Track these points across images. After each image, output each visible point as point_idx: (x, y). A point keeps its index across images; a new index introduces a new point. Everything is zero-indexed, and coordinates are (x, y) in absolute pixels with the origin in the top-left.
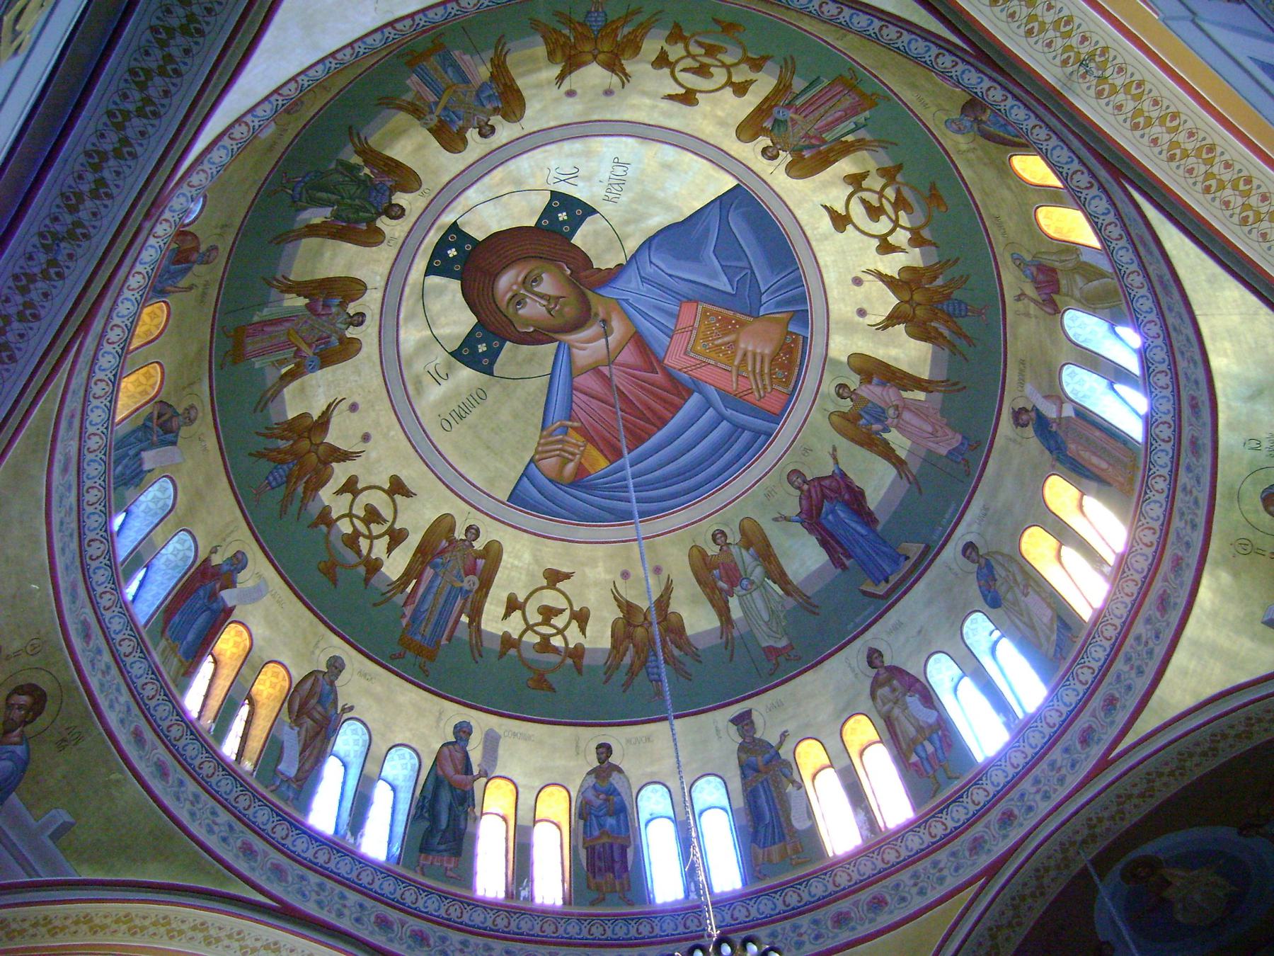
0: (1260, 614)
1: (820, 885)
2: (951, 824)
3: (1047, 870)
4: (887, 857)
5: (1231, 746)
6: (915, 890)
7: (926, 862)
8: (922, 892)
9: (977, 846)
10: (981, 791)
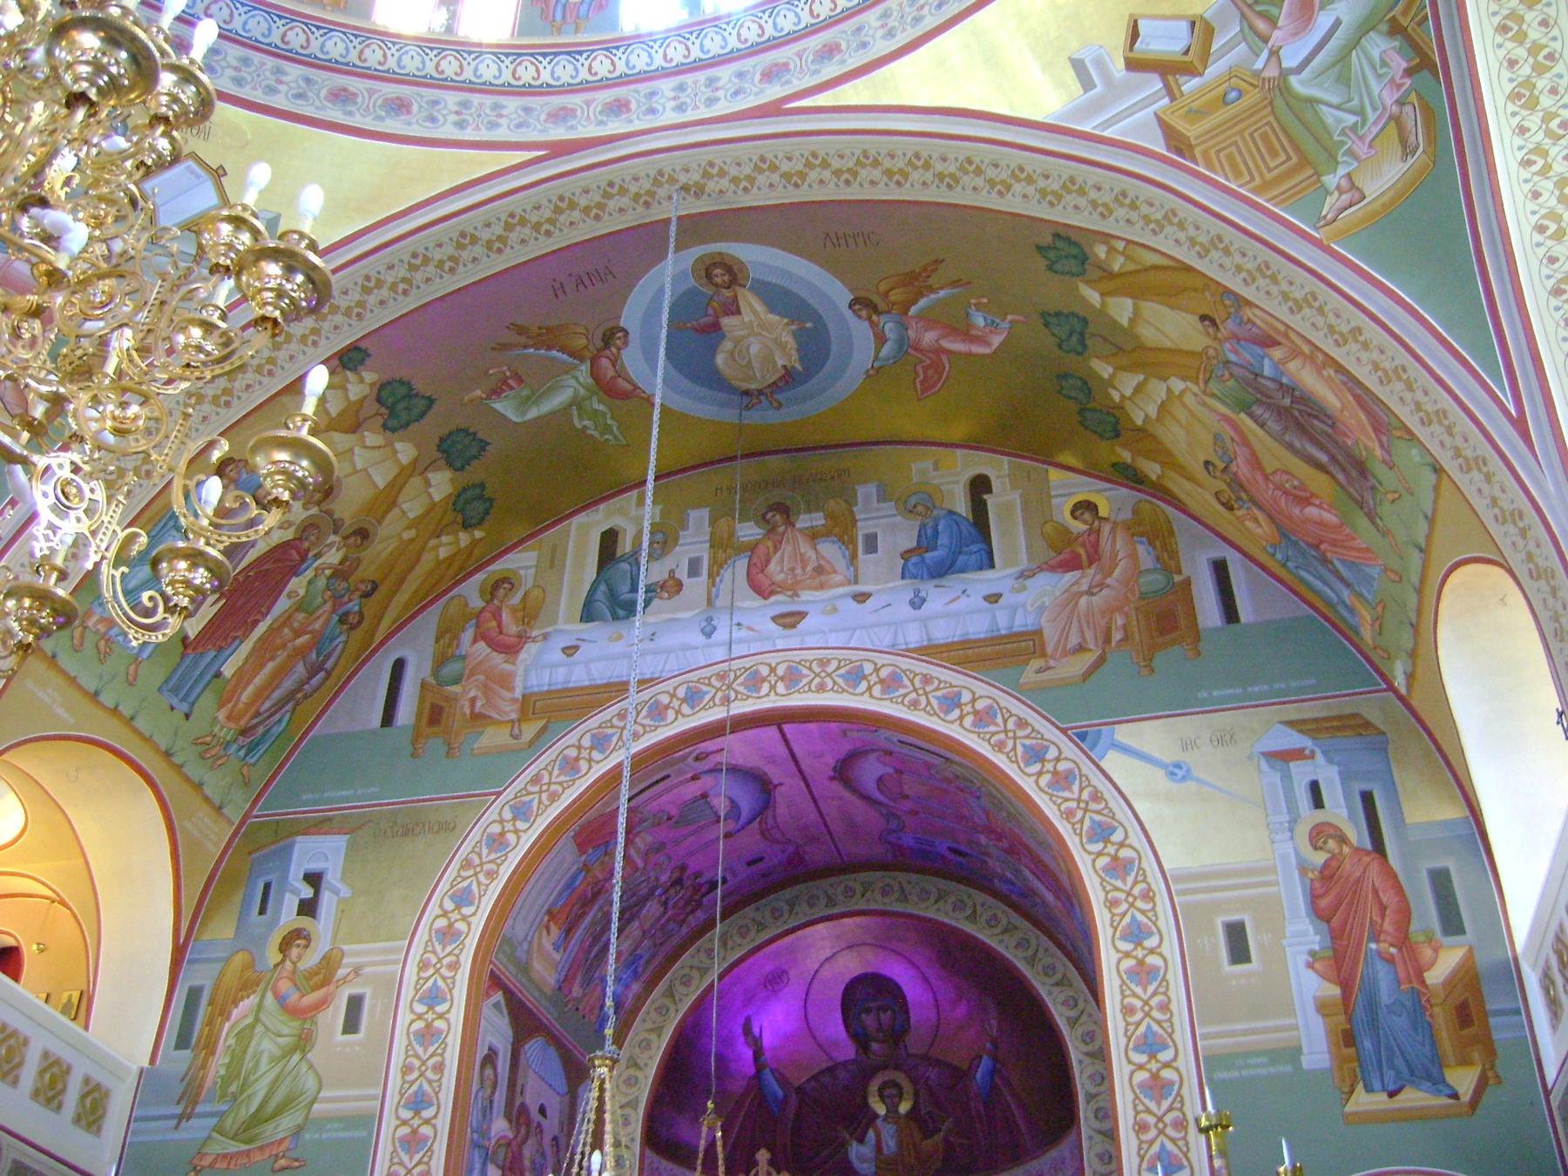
0: (1074, 47)
1: (341, 46)
2: (546, 77)
3: (623, 191)
4: (444, 65)
5: (924, 183)
6: (454, 118)
7: (489, 100)
8: (461, 125)
9: (561, 115)
10: (607, 63)
